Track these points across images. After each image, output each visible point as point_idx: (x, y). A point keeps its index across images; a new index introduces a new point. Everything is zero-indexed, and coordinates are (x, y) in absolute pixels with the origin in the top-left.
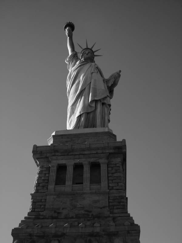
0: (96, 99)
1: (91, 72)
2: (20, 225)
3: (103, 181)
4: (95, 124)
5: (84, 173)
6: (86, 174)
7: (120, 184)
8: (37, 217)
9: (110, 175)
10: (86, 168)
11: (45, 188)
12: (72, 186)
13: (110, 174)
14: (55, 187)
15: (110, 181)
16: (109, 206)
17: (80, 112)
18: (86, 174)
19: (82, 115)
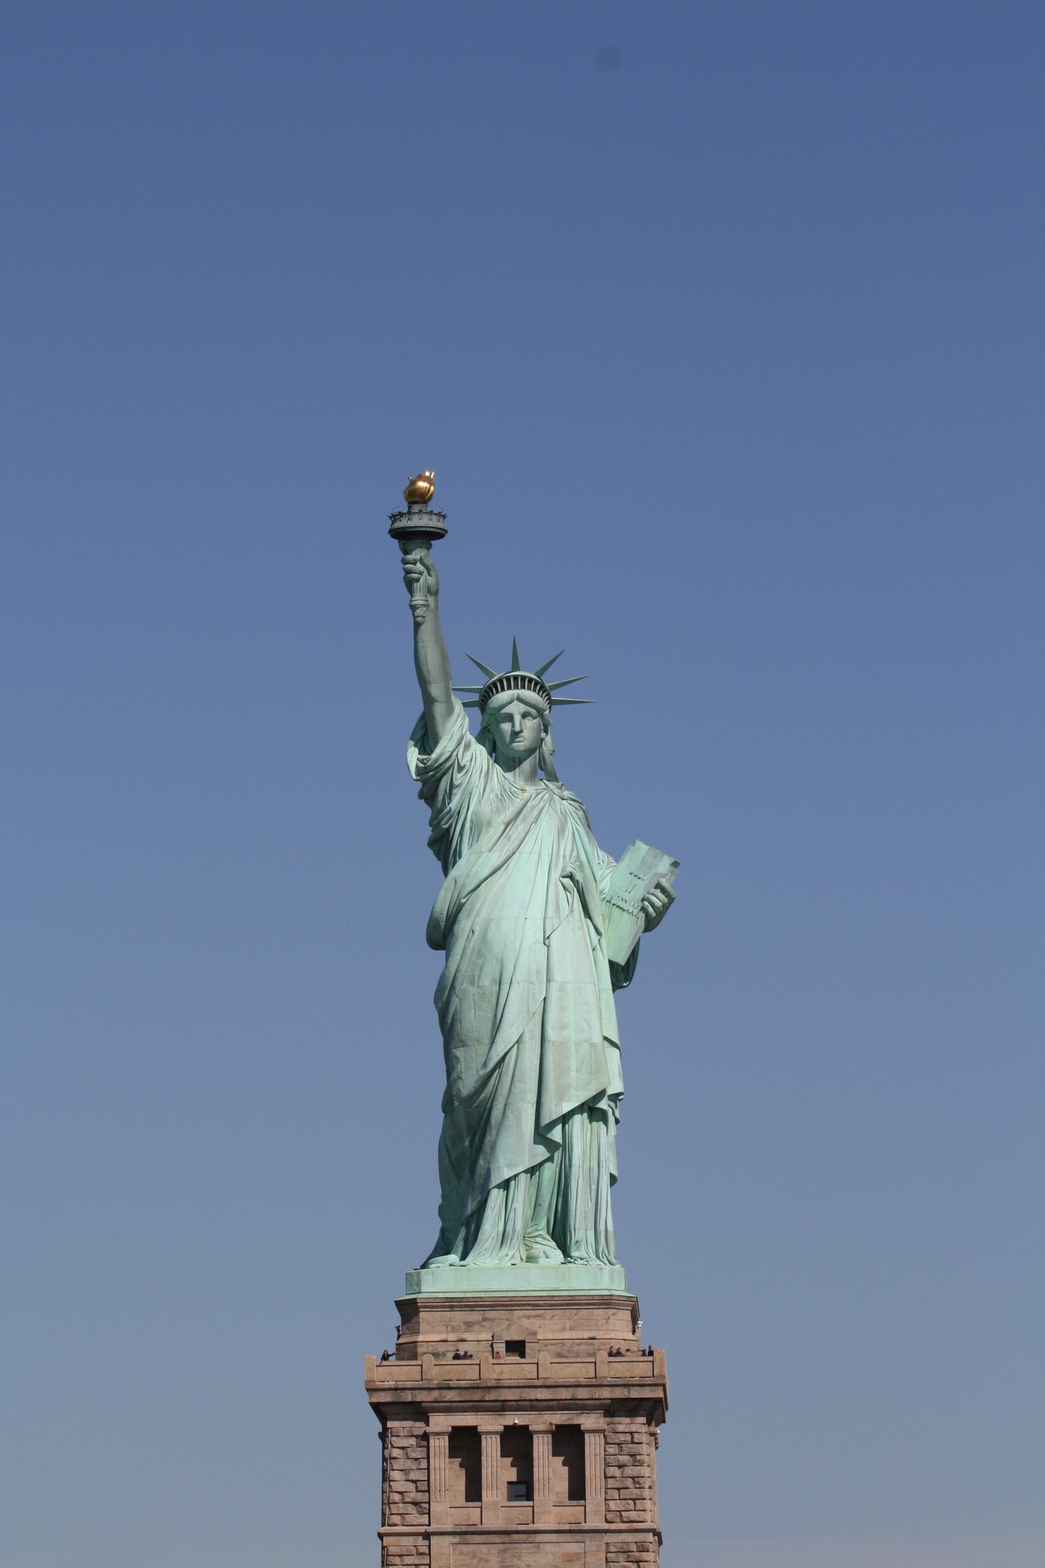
0: (567, 1107)
5: (535, 1463)
6: (541, 1468)
13: (612, 1469)
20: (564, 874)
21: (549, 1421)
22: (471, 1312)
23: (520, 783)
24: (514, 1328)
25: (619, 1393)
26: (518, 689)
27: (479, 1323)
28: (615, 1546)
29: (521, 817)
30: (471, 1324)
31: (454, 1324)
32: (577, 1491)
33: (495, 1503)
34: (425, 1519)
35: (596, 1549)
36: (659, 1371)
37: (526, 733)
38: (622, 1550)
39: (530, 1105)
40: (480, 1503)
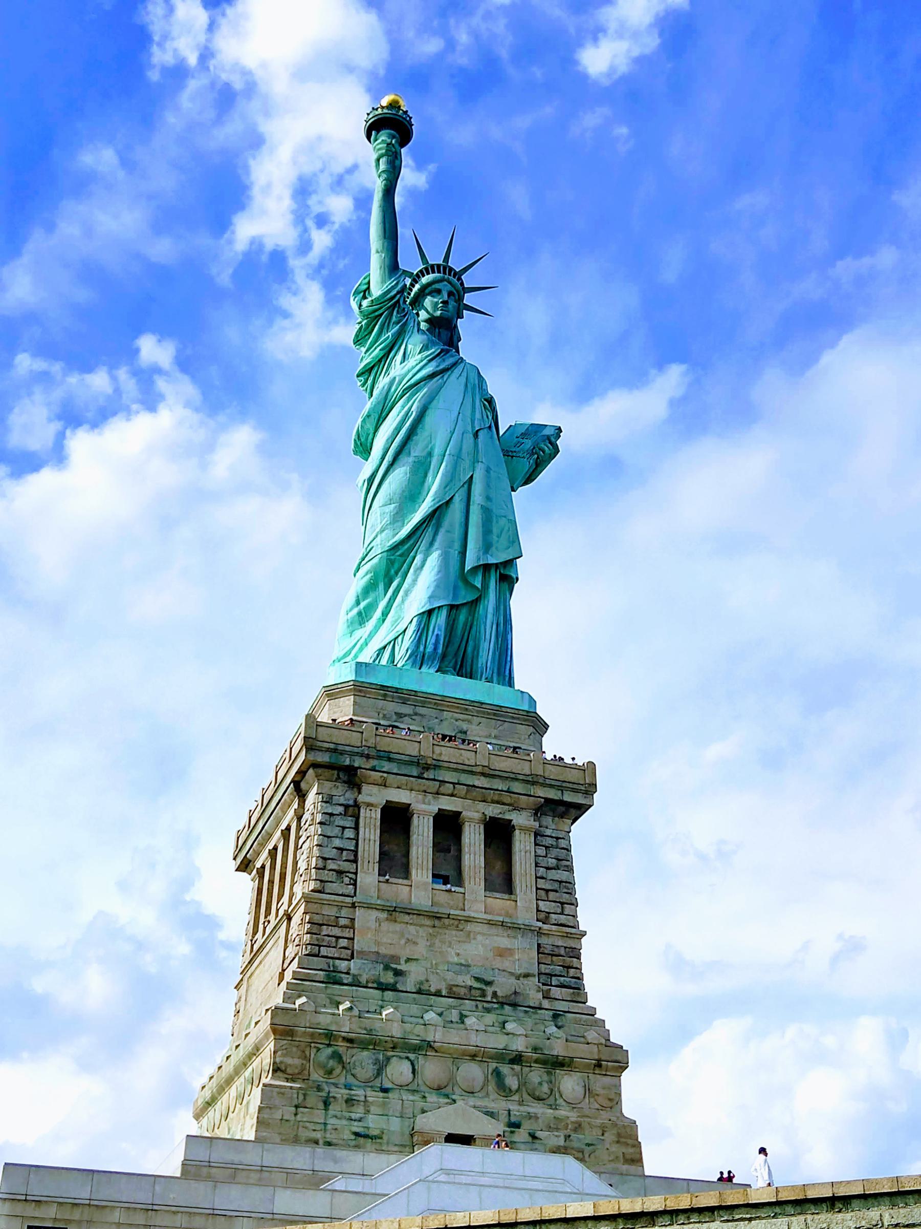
1: (473, 427)
4: (470, 649)
5: (467, 850)
6: (472, 855)
8: (333, 978)
10: (472, 834)
13: (541, 869)
15: (542, 893)
18: (472, 855)
19: (436, 611)
21: (483, 811)
22: (403, 705)
24: (445, 723)
25: (553, 794)
27: (409, 715)
30: (402, 716)
32: (507, 886)
33: (426, 884)
35: (528, 947)
36: (591, 780)
38: (551, 952)
39: (457, 552)
40: (410, 882)
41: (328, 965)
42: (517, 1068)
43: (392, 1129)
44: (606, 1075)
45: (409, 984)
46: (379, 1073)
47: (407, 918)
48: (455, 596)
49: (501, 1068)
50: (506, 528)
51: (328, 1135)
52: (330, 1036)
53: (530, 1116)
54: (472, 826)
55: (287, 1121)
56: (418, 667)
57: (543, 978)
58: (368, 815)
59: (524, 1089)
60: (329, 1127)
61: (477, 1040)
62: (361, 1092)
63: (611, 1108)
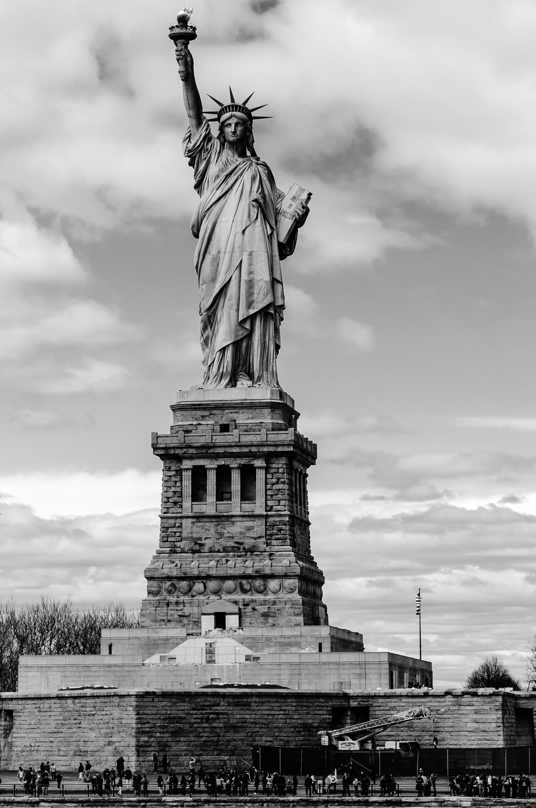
0: (252, 311)
2: (153, 563)
3: (259, 496)
5: (232, 483)
6: (235, 485)
7: (282, 503)
8: (173, 551)
9: (269, 486)
10: (235, 475)
11: (178, 505)
12: (216, 504)
14: (192, 505)
15: (269, 497)
16: (266, 535)
17: (224, 340)
18: (235, 485)
19: (227, 347)
20: (253, 200)
23: (236, 156)
24: (224, 418)
25: (271, 449)
26: (234, 111)
27: (208, 416)
28: (270, 523)
29: (234, 173)
31: (196, 417)
34: (180, 510)
36: (291, 438)
37: (238, 132)
39: (235, 311)
41: (172, 544)
42: (250, 581)
43: (194, 612)
44: (290, 579)
45: (206, 548)
46: (190, 589)
47: (205, 520)
48: (236, 336)
49: (242, 582)
50: (263, 287)
51: (168, 617)
52: (169, 578)
53: (253, 601)
54: (235, 471)
55: (153, 613)
56: (218, 381)
57: (269, 537)
58: (185, 474)
59: (253, 589)
60: (169, 614)
61: (231, 572)
62: (182, 598)
63: (292, 592)
